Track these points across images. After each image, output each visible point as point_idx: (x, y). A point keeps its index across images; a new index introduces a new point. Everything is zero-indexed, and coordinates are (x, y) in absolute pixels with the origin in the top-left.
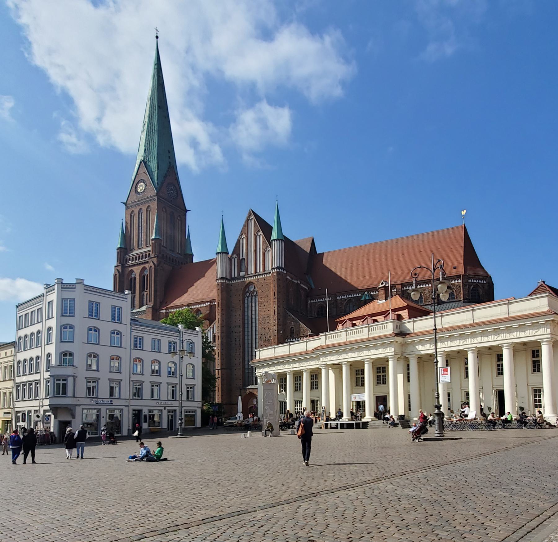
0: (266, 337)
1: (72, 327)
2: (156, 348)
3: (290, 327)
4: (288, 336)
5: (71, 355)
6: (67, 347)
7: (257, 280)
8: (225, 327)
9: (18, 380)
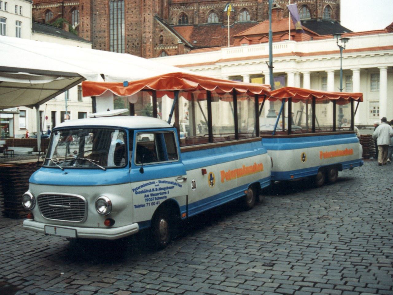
3: (159, 36)
4: (157, 44)
8: (89, 31)
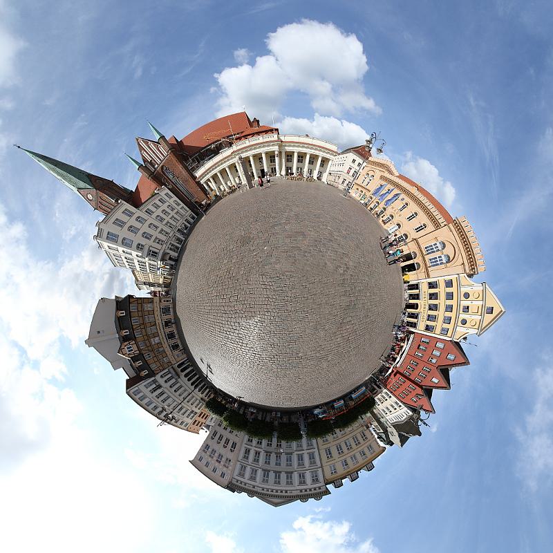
1: (124, 239)
2: (157, 207)
5: (139, 245)
6: (135, 245)
9: (148, 271)
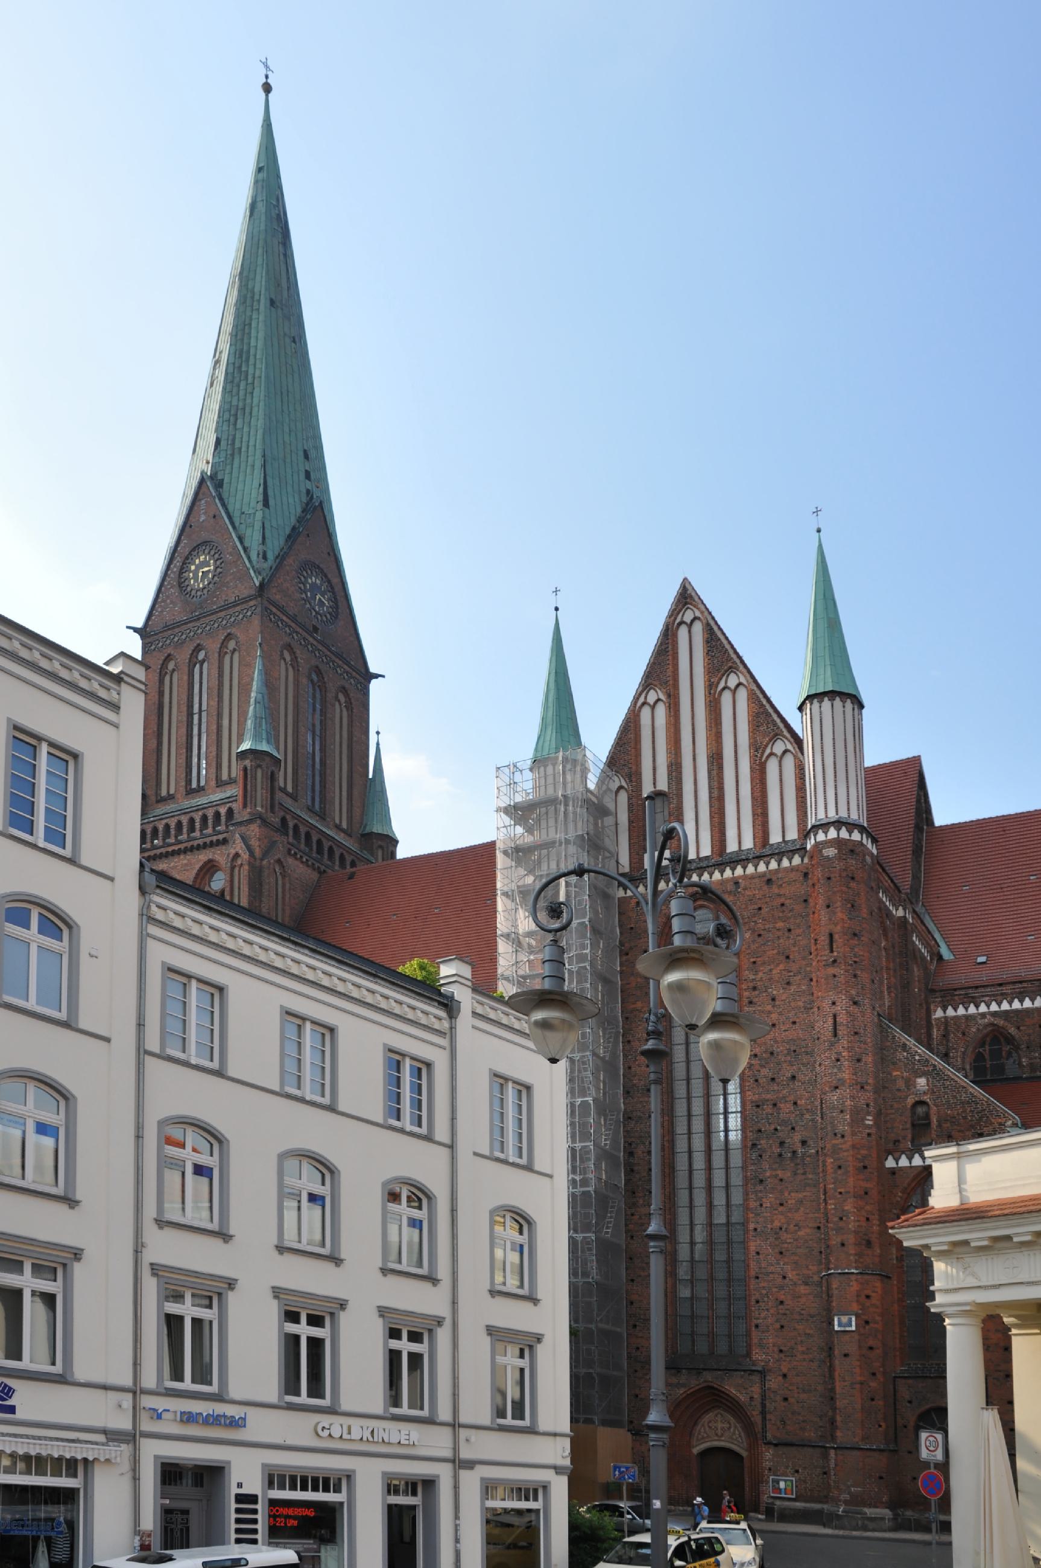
0: (782, 1143)
3: (910, 1101)
4: (896, 1142)
7: (730, 887)
